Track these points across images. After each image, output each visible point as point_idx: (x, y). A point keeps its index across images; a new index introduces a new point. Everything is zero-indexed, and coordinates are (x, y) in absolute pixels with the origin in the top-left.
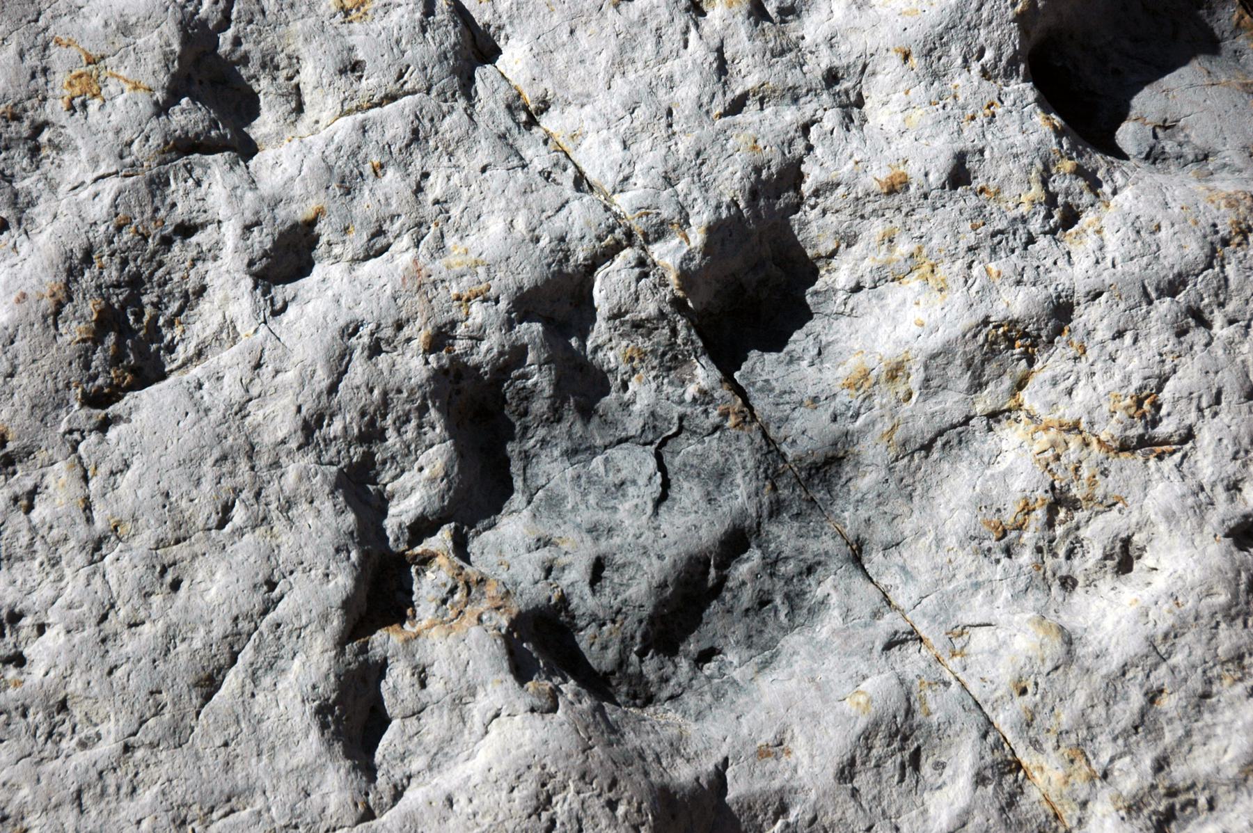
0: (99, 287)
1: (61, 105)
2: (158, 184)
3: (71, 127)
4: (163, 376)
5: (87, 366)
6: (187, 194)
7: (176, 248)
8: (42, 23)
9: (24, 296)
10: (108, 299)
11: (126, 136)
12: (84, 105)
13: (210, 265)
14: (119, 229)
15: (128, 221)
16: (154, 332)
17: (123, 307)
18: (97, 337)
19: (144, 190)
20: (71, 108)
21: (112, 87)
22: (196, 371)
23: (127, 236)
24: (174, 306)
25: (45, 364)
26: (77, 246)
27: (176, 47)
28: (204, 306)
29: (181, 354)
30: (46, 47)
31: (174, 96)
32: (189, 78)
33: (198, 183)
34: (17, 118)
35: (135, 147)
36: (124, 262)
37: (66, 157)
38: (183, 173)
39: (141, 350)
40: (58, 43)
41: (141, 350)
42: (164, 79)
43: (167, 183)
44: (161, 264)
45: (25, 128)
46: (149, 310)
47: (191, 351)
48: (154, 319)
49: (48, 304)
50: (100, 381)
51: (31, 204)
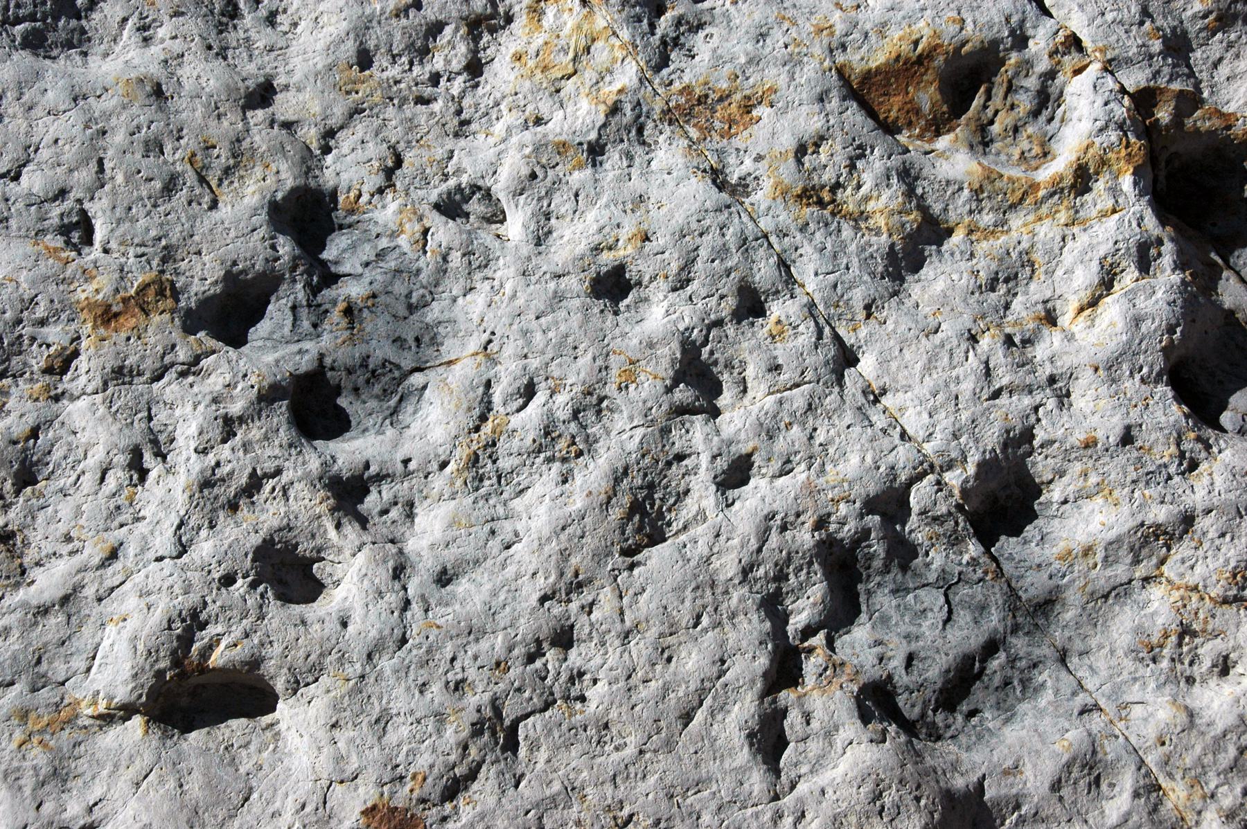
0: (631, 489)
1: (614, 387)
2: (665, 431)
3: (620, 399)
4: (665, 540)
5: (623, 533)
6: (681, 437)
7: (674, 467)
8: (606, 342)
9: (590, 493)
10: (635, 496)
11: (649, 405)
12: (627, 387)
13: (692, 477)
14: (643, 456)
15: (648, 452)
16: (661, 515)
17: (644, 500)
18: (629, 517)
19: (657, 433)
20: (620, 389)
21: (642, 377)
22: (683, 538)
23: (647, 460)
24: (672, 501)
25: (601, 531)
26: (620, 465)
27: (678, 355)
28: (688, 501)
29: (675, 527)
30: (608, 355)
31: (676, 383)
32: (684, 373)
33: (687, 431)
34: (590, 394)
35: (654, 410)
36: (645, 475)
37: (616, 416)
38: (679, 425)
39: (653, 525)
40: (614, 352)
41: (653, 525)
42: (671, 373)
43: (670, 431)
44: (665, 476)
45: (594, 399)
46: (658, 502)
47: (681, 526)
48: (661, 507)
49: (603, 497)
50: (630, 542)
51: (596, 441)
